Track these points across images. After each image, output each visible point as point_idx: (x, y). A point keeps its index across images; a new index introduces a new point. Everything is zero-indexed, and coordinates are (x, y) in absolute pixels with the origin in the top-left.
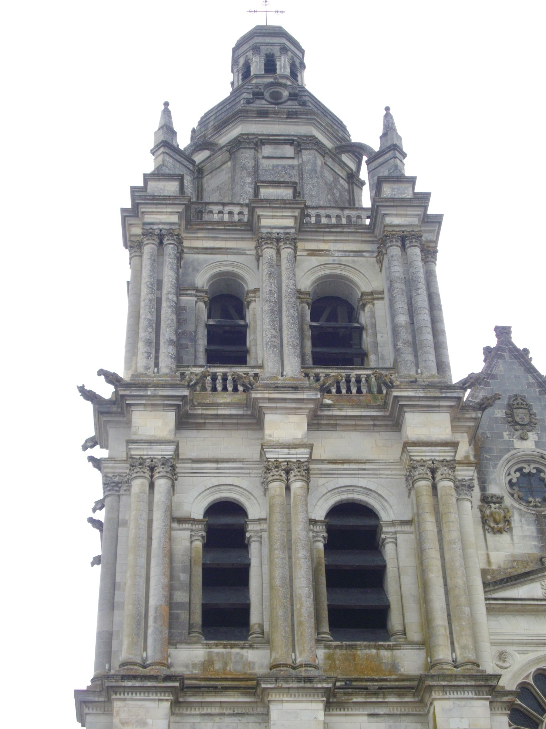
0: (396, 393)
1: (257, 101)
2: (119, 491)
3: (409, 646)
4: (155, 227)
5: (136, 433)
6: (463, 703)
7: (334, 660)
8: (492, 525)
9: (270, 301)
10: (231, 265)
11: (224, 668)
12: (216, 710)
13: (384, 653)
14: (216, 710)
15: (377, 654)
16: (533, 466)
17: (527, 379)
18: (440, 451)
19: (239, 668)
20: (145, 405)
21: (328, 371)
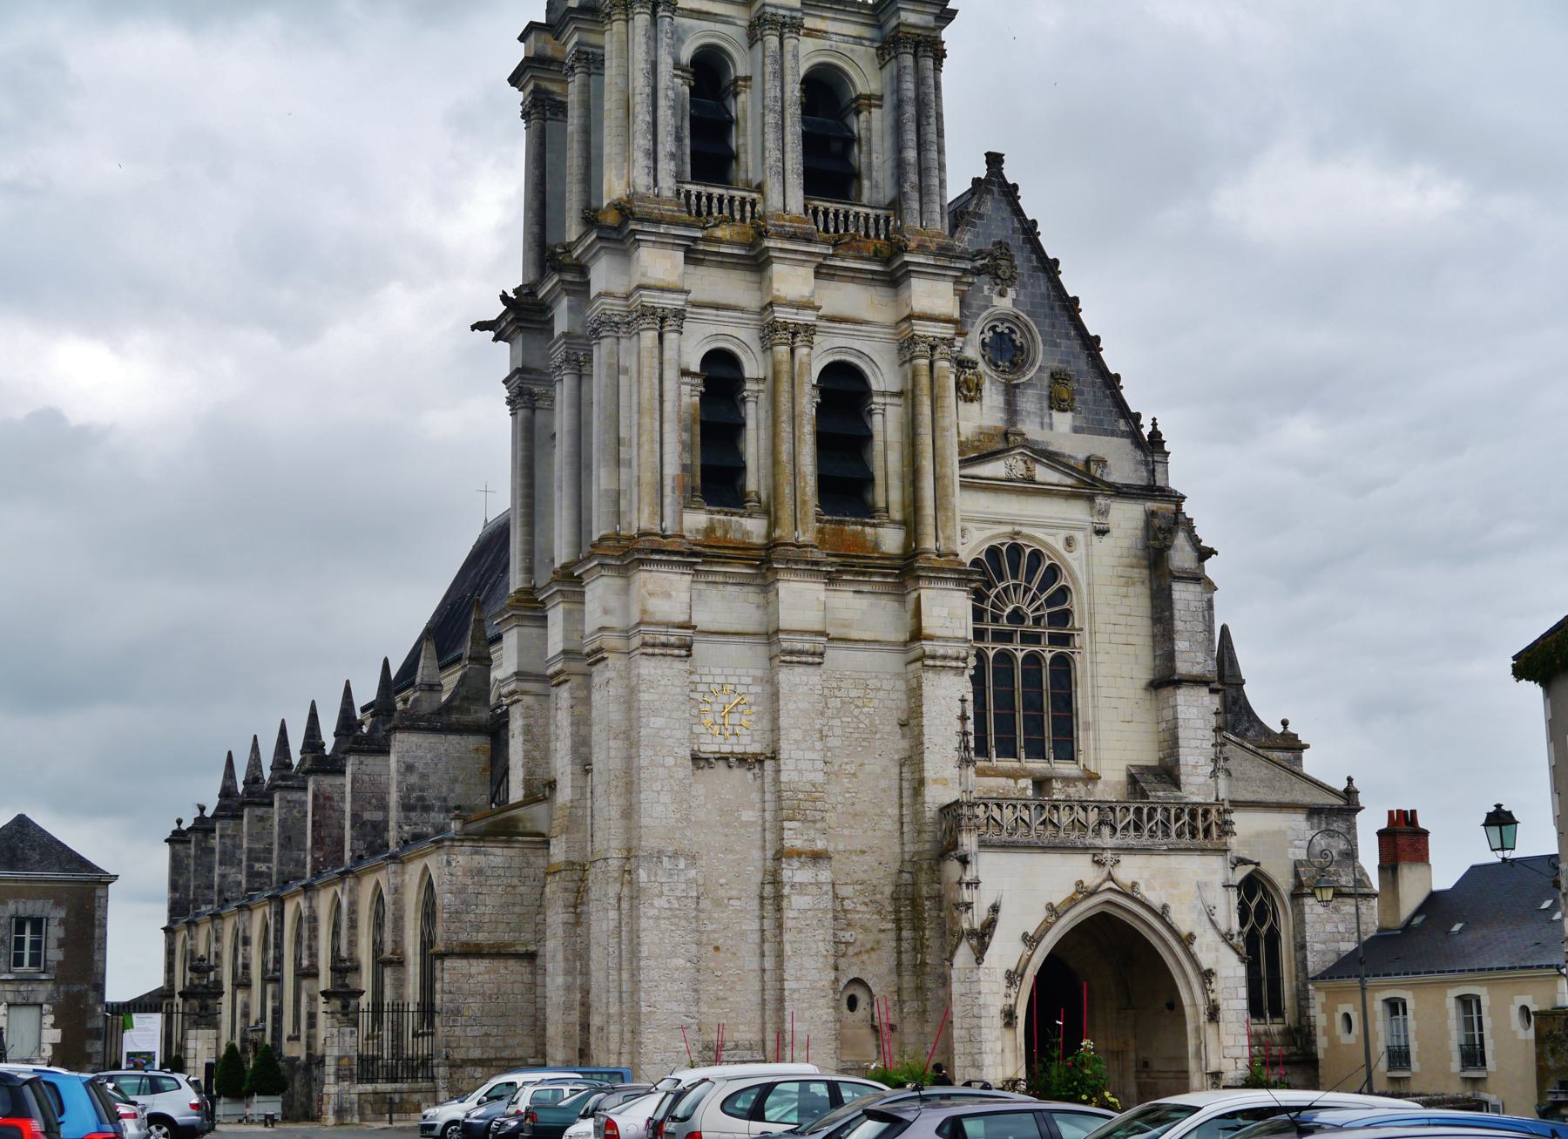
2: (617, 332)
3: (892, 526)
5: (644, 275)
6: (945, 592)
7: (823, 534)
8: (965, 392)
10: (719, 37)
11: (725, 536)
12: (720, 579)
13: (868, 530)
15: (863, 530)
16: (1006, 325)
17: (1013, 223)
18: (942, 328)
19: (739, 536)
20: (654, 242)
21: (828, 205)
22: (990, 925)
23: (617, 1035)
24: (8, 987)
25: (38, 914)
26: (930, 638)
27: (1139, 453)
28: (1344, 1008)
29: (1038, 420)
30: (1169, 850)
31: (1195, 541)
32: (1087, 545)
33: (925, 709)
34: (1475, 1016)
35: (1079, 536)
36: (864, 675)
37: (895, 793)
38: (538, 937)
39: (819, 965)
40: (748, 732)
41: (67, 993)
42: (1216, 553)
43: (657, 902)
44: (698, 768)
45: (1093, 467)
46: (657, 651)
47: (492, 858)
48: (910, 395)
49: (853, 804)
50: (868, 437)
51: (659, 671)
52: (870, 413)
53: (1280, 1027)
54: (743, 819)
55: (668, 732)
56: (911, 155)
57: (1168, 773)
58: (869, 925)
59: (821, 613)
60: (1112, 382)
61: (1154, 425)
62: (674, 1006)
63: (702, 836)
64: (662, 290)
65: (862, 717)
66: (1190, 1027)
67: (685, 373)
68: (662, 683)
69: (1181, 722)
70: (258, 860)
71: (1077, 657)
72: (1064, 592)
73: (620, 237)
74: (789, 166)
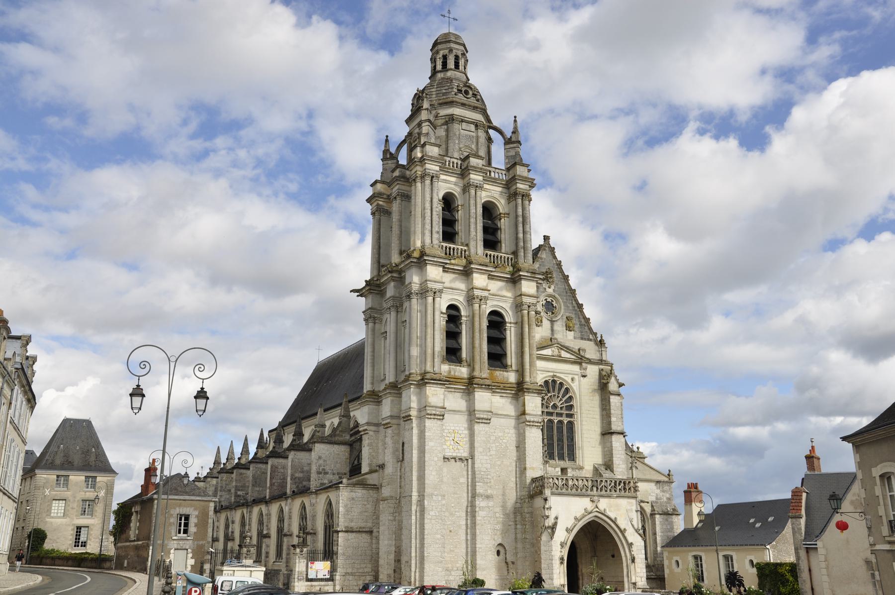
1: (459, 94)
4: (430, 171)
13: (505, 373)
14: (453, 390)
16: (551, 298)
19: (459, 374)
21: (491, 252)
22: (555, 524)
24: (175, 542)
25: (187, 513)
27: (597, 347)
28: (675, 558)
29: (562, 334)
30: (617, 497)
31: (617, 380)
32: (579, 381)
33: (526, 441)
34: (730, 563)
35: (576, 377)
36: (504, 428)
37: (514, 473)
38: (374, 525)
39: (489, 539)
41: (197, 544)
42: (624, 385)
44: (444, 462)
45: (581, 352)
46: (432, 417)
48: (520, 324)
49: (499, 476)
50: (504, 339)
51: (432, 425)
52: (505, 330)
56: (521, 235)
57: (609, 466)
59: (490, 404)
61: (601, 337)
63: (446, 488)
64: (435, 282)
65: (503, 443)
66: (625, 565)
67: (442, 313)
69: (614, 448)
70: (239, 490)
71: (575, 423)
72: (571, 398)
73: (419, 262)
74: (478, 238)
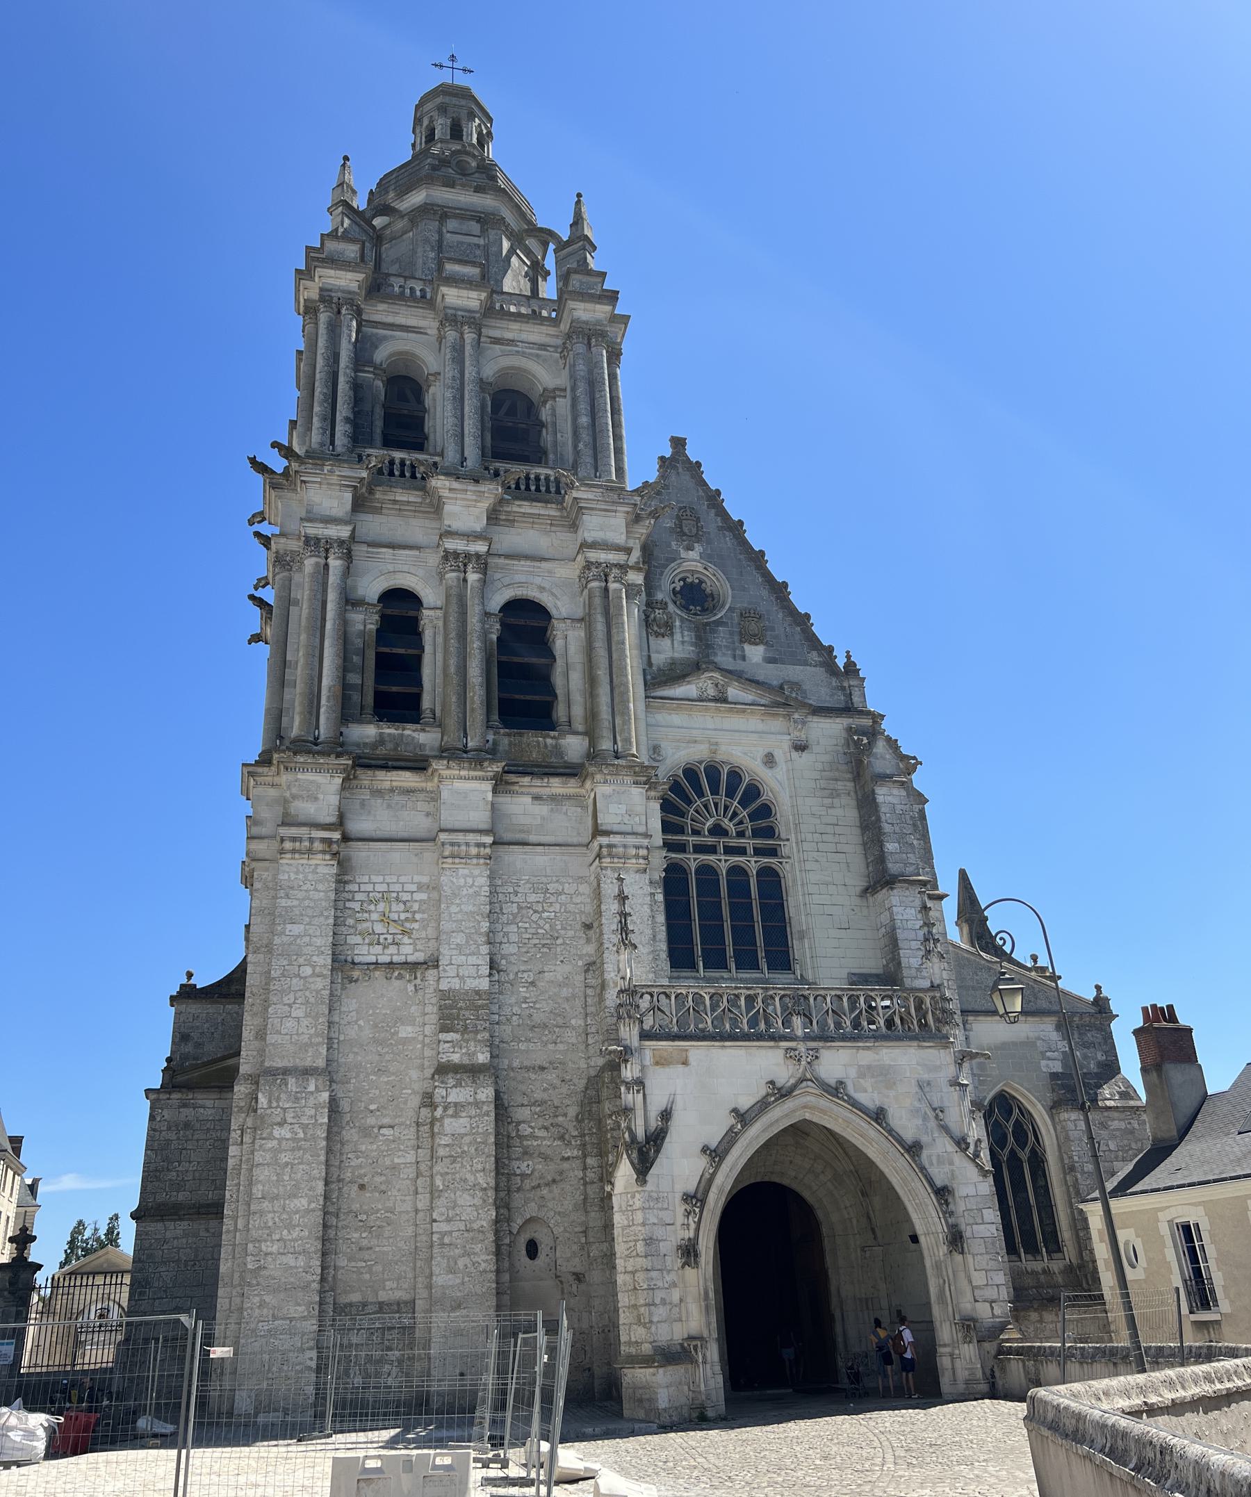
0: (575, 494)
8: (656, 628)
9: (453, 388)
13: (549, 741)
23: (227, 1300)
26: (607, 833)
36: (544, 880)
37: (578, 1003)
40: (411, 941)
43: (277, 1132)
47: (202, 1110)
51: (301, 876)
53: (1061, 1266)
54: (400, 1035)
55: (307, 939)
57: (890, 978)
58: (549, 1152)
59: (488, 814)
60: (803, 621)
61: (848, 657)
62: (290, 1260)
65: (541, 922)
68: (305, 888)
69: (898, 923)
